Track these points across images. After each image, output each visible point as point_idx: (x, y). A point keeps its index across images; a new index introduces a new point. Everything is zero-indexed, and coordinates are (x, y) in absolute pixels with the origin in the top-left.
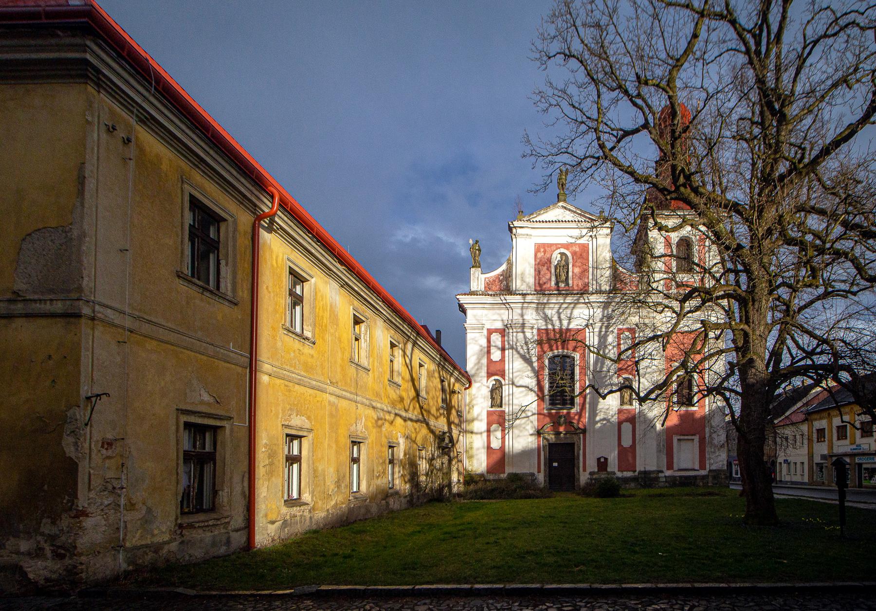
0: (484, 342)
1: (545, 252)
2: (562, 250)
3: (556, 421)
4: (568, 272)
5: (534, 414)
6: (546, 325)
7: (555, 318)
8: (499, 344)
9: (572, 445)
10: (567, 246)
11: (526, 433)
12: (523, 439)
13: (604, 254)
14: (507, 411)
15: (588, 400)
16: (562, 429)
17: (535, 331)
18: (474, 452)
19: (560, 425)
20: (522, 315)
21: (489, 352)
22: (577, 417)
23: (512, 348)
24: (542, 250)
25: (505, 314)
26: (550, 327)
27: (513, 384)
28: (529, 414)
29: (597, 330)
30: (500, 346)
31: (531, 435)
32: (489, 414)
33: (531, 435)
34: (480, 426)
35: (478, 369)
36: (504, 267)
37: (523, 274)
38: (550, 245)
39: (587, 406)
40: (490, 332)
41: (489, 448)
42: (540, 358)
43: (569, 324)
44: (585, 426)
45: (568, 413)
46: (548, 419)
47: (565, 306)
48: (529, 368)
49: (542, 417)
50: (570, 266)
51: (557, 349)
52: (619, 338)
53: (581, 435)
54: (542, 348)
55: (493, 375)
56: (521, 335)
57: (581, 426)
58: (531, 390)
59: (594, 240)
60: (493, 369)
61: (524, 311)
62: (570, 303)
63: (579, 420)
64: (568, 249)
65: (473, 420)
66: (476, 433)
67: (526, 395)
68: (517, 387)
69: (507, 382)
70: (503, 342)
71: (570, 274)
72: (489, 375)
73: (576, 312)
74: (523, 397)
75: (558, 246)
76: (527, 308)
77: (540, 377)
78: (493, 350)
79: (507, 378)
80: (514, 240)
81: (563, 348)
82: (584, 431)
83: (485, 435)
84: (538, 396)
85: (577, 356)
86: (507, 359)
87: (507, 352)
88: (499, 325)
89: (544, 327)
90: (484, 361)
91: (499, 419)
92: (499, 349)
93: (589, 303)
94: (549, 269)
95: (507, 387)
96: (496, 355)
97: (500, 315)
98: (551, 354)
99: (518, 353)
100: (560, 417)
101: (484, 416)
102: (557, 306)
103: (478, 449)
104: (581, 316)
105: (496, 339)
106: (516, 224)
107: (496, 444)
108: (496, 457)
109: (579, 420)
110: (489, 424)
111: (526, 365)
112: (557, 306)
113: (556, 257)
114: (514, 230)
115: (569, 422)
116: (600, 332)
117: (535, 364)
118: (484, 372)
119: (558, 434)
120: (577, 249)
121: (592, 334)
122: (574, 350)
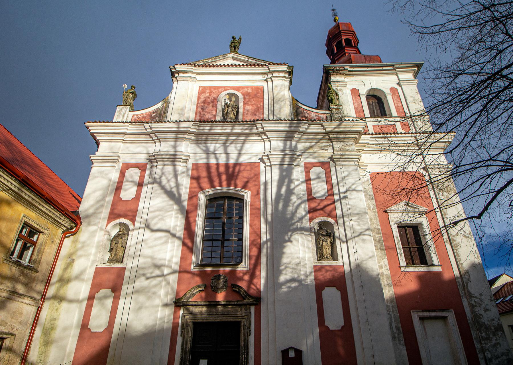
0: (115, 176)
1: (211, 93)
2: (231, 91)
3: (210, 284)
4: (237, 112)
5: (174, 272)
6: (208, 158)
7: (220, 151)
8: (137, 179)
9: (237, 325)
10: (238, 88)
11: (157, 302)
12: (148, 310)
13: (282, 93)
14: (129, 266)
15: (264, 251)
16: (221, 297)
17: (190, 166)
18: (56, 334)
19: (216, 290)
20: (175, 147)
21: (118, 188)
22: (246, 277)
23: (154, 181)
24: (208, 91)
25: (153, 148)
26: (213, 161)
27: (148, 227)
28: (166, 271)
29: (276, 162)
30: (138, 181)
31: (166, 305)
32: (98, 272)
33: (166, 305)
34: (81, 289)
35: (97, 209)
36: (159, 105)
37: (182, 109)
38: (219, 87)
39: (263, 259)
40: (127, 166)
41: (84, 326)
42: (192, 196)
43: (239, 155)
44: (259, 291)
45: (233, 273)
46: (198, 280)
47: (232, 138)
48: (175, 207)
49: (187, 276)
50: (241, 104)
51: (221, 185)
52: (307, 173)
53: (253, 309)
54: (199, 184)
55: (120, 216)
56: (169, 169)
57: (252, 291)
58: (174, 236)
59: (270, 83)
60: (120, 209)
61: (178, 143)
62: (240, 134)
63: (250, 282)
64: (238, 90)
65: (68, 281)
66: (71, 301)
67: (166, 242)
68: (153, 231)
69: (137, 225)
70: (142, 177)
71: (241, 110)
72: (113, 215)
73: (248, 146)
74: (161, 245)
75: (225, 88)
76: (183, 138)
77: (191, 219)
78: (126, 185)
79: (138, 219)
80: (175, 84)
81: (229, 185)
82: (257, 300)
83: (85, 303)
84: (184, 244)
85: (247, 195)
86: (143, 196)
87: (144, 189)
88: (142, 159)
89: (205, 161)
90: (110, 199)
91: (111, 282)
92: (135, 184)
93: (264, 133)
94: (215, 106)
95: (136, 232)
96: (128, 193)
97: (146, 148)
98: (210, 191)
99: (163, 188)
100: (218, 277)
101: (90, 274)
102: (223, 138)
103: (65, 329)
104: (253, 150)
105: (134, 174)
106: (178, 68)
107: (99, 321)
108: (92, 348)
109: (250, 282)
110: (96, 287)
111: (171, 202)
112: (223, 138)
113: (223, 97)
114: (176, 75)
115: (233, 288)
116: (281, 165)
117: (185, 203)
118: (105, 212)
119: (212, 304)
120: (250, 90)
121: (268, 168)
122: (244, 187)
